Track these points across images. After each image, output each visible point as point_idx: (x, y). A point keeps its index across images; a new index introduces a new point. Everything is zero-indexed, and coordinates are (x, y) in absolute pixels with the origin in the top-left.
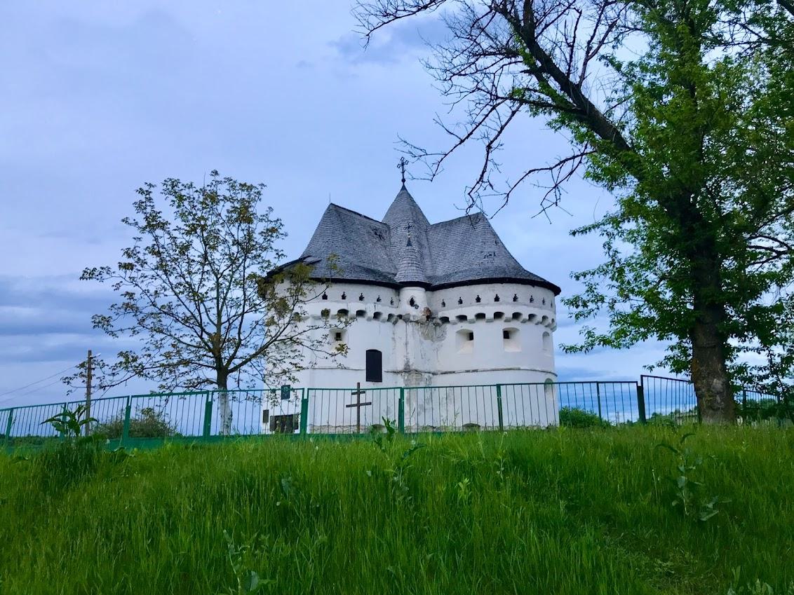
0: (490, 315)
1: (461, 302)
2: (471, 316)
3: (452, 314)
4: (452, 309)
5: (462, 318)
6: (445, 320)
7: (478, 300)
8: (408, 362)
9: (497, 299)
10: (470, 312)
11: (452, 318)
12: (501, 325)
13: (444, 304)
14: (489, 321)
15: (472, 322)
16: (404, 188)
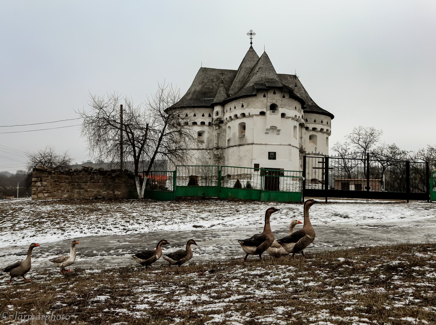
0: (325, 130)
1: (315, 121)
2: (319, 129)
3: (311, 126)
4: (312, 124)
5: (314, 129)
6: (307, 128)
7: (322, 122)
8: (302, 147)
9: (327, 123)
10: (319, 127)
11: (311, 128)
12: (326, 135)
13: (307, 121)
14: (324, 133)
15: (318, 132)
16: (251, 47)
